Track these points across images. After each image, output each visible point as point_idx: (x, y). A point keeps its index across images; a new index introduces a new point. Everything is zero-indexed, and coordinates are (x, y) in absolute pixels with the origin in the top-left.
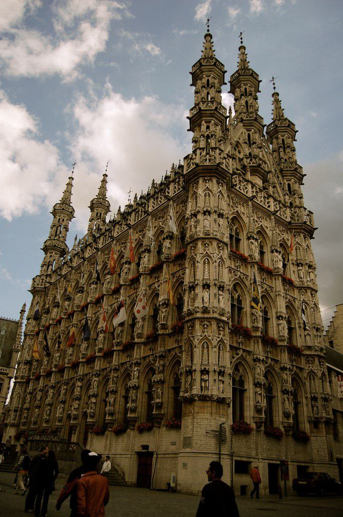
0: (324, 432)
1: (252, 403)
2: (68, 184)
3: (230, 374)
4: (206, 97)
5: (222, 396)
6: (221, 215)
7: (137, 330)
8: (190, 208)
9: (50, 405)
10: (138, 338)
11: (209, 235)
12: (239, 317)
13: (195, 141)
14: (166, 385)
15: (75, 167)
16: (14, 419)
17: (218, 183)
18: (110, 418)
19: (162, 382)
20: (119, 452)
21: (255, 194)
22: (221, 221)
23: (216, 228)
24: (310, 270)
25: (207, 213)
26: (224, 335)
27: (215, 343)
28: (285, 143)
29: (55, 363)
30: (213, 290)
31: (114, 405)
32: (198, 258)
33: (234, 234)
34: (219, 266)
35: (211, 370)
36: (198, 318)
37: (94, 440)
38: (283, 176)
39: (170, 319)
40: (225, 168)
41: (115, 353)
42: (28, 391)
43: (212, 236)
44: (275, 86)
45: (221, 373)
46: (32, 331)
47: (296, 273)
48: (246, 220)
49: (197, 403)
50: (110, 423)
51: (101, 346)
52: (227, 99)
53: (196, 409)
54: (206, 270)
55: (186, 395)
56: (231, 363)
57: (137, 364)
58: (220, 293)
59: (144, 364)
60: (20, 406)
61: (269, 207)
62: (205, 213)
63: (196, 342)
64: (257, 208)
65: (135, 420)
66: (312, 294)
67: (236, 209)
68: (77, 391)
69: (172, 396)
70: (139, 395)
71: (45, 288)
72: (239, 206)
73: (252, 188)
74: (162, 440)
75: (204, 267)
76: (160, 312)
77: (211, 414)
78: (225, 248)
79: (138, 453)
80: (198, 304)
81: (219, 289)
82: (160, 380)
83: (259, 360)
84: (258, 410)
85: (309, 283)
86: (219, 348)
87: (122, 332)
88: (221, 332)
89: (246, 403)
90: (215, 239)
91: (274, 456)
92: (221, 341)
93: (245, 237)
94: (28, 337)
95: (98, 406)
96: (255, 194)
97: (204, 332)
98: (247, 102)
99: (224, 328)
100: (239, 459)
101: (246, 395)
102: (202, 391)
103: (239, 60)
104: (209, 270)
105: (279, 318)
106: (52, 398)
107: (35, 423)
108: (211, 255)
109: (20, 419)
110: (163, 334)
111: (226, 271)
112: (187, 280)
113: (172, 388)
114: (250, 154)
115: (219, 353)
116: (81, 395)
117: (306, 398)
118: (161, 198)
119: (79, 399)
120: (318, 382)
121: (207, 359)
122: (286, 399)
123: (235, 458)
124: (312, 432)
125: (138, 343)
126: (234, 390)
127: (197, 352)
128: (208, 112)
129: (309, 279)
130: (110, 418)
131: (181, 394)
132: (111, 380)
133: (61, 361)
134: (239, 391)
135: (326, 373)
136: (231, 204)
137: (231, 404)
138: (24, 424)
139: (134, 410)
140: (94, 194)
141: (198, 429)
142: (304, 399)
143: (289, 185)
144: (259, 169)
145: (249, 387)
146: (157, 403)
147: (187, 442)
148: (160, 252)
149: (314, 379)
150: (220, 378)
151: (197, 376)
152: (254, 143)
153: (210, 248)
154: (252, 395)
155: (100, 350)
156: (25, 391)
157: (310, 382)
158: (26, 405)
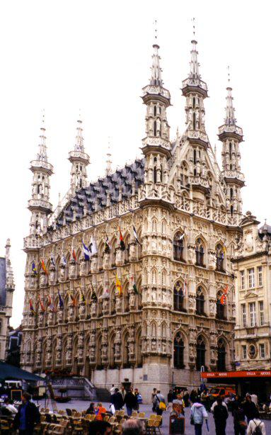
5: (164, 353)
6: (164, 238)
9: (60, 351)
14: (136, 344)
16: (29, 360)
19: (134, 343)
22: (165, 242)
23: (160, 248)
27: (159, 323)
30: (159, 292)
32: (149, 269)
35: (158, 338)
36: (149, 309)
46: (32, 288)
57: (119, 329)
59: (124, 329)
60: (32, 350)
63: (148, 323)
64: (197, 220)
68: (80, 343)
70: (122, 349)
71: (38, 249)
78: (168, 261)
79: (124, 384)
84: (191, 359)
87: (108, 304)
92: (164, 321)
94: (29, 294)
95: (97, 353)
96: (196, 209)
106: (61, 345)
107: (49, 363)
133: (64, 316)
138: (39, 364)
139: (119, 358)
147: (145, 377)
156: (35, 338)
158: (38, 350)
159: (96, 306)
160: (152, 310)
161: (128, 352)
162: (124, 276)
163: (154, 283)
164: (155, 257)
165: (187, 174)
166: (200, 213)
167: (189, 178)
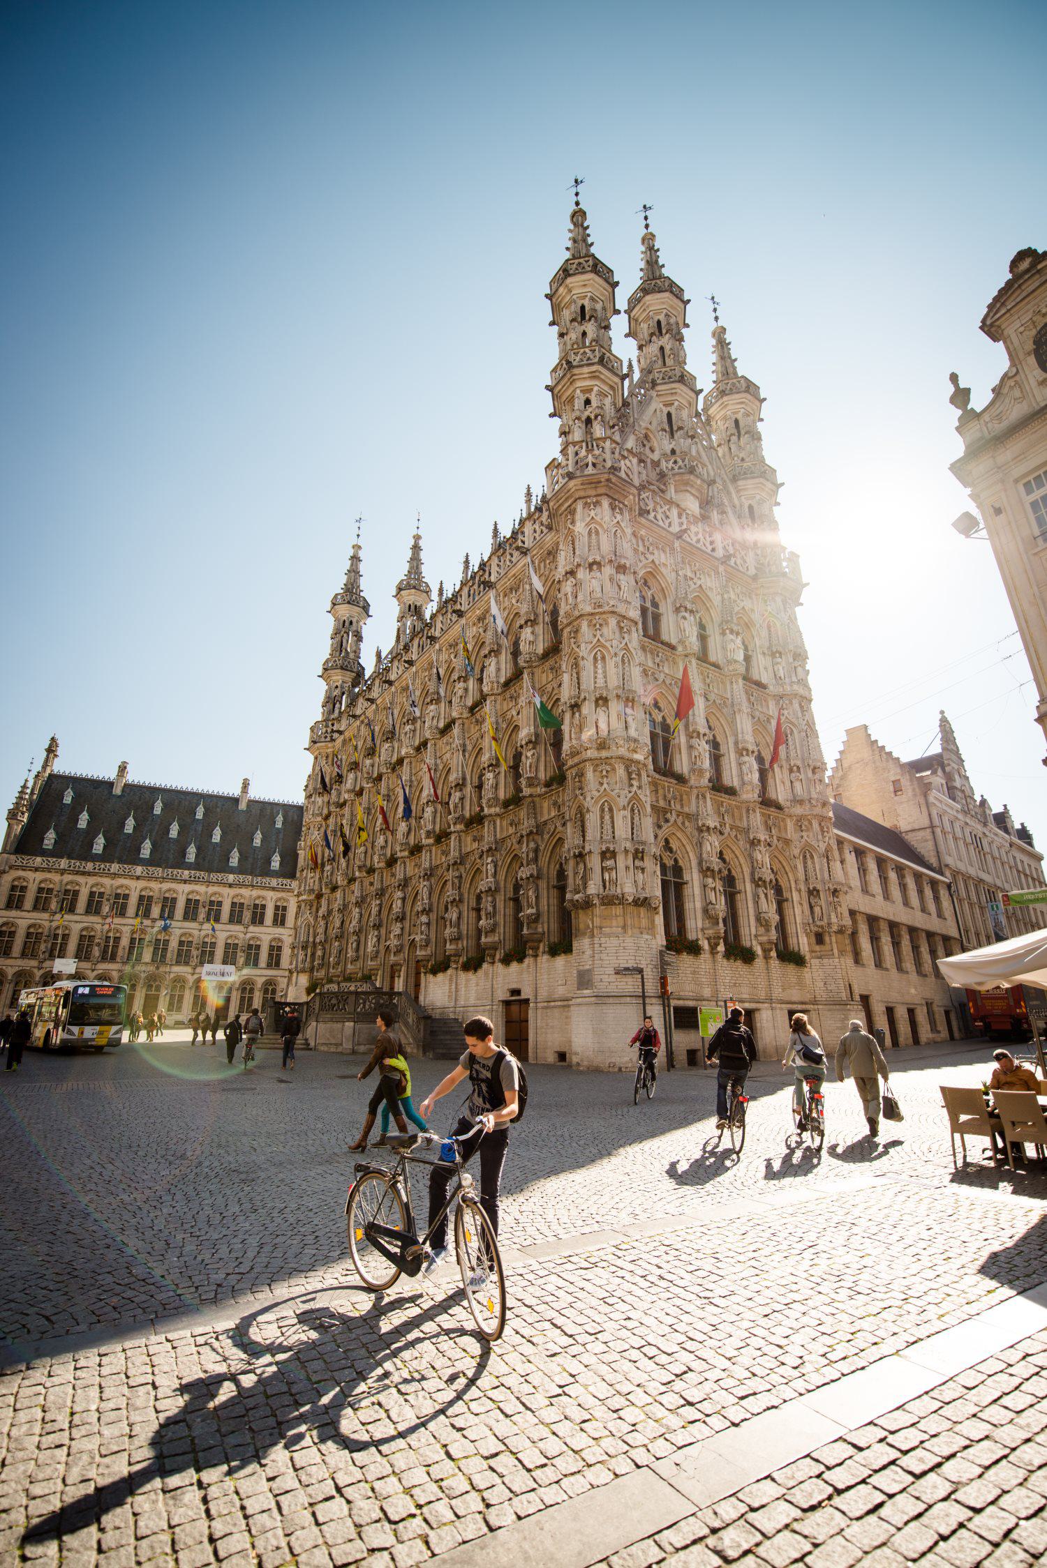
0: (836, 951)
1: (698, 905)
2: (352, 558)
3: (655, 856)
4: (580, 341)
6: (621, 569)
7: (487, 793)
8: (563, 562)
10: (490, 807)
11: (600, 606)
12: (666, 755)
13: (563, 433)
14: (543, 884)
15: (361, 525)
16: (304, 961)
17: (613, 509)
18: (453, 947)
20: (472, 1001)
21: (684, 527)
24: (796, 664)
25: (595, 567)
26: (640, 787)
27: (623, 801)
28: (741, 424)
29: (358, 863)
31: (458, 925)
32: (584, 651)
33: (648, 604)
34: (623, 661)
35: (619, 849)
37: (431, 985)
38: (738, 491)
39: (542, 768)
40: (624, 476)
41: (453, 837)
42: (320, 914)
43: (606, 608)
44: (718, 313)
45: (639, 855)
47: (770, 669)
48: (671, 577)
49: (597, 911)
50: (455, 955)
51: (430, 827)
52: (624, 349)
53: (597, 921)
54: (600, 671)
55: (577, 897)
56: (656, 837)
58: (629, 711)
60: (311, 940)
61: (713, 550)
62: (591, 565)
63: (588, 803)
65: (494, 948)
66: (801, 707)
67: (651, 558)
69: (554, 901)
70: (500, 905)
72: (656, 552)
73: (680, 516)
74: (543, 976)
75: (596, 667)
76: (523, 758)
77: (624, 927)
78: (634, 629)
79: (507, 1003)
80: (588, 734)
81: (626, 706)
82: (532, 876)
83: (708, 828)
85: (795, 687)
86: (632, 810)
87: (462, 799)
88: (635, 783)
89: (688, 906)
90: (613, 612)
91: (745, 996)
93: (670, 609)
95: (433, 928)
97: (602, 784)
98: (662, 348)
99: (639, 775)
100: (681, 1003)
101: (687, 891)
102: (605, 887)
103: (642, 265)
104: (605, 672)
105: (741, 752)
106: (360, 921)
108: (608, 644)
109: (313, 960)
110: (531, 796)
111: (636, 672)
112: (566, 694)
113: (554, 887)
114: (673, 452)
115: (632, 819)
116: (404, 913)
117: (799, 891)
118: (511, 555)
119: (401, 918)
120: (819, 863)
121: (610, 832)
122: (762, 896)
123: (673, 1003)
124: (812, 951)
125: (490, 815)
126: (665, 884)
127: (592, 820)
128: (586, 370)
129: (794, 679)
130: (453, 947)
131: (568, 896)
132: (450, 883)
134: (673, 885)
135: (835, 847)
136: (641, 549)
137: (661, 909)
139: (493, 930)
140: (400, 571)
141: (604, 956)
142: (795, 895)
143: (751, 507)
144: (692, 477)
145: (693, 878)
146: (529, 916)
147: (584, 980)
148: (516, 653)
149: (812, 857)
150: (638, 863)
151: (595, 862)
152: (680, 428)
153: (605, 630)
154: (697, 891)
155: (428, 834)
157: (805, 863)
159: (435, 812)
160: (597, 763)
161: (518, 907)
162: (504, 715)
163: (600, 682)
164: (597, 616)
165: (656, 457)
166: (695, 539)
167: (664, 464)
